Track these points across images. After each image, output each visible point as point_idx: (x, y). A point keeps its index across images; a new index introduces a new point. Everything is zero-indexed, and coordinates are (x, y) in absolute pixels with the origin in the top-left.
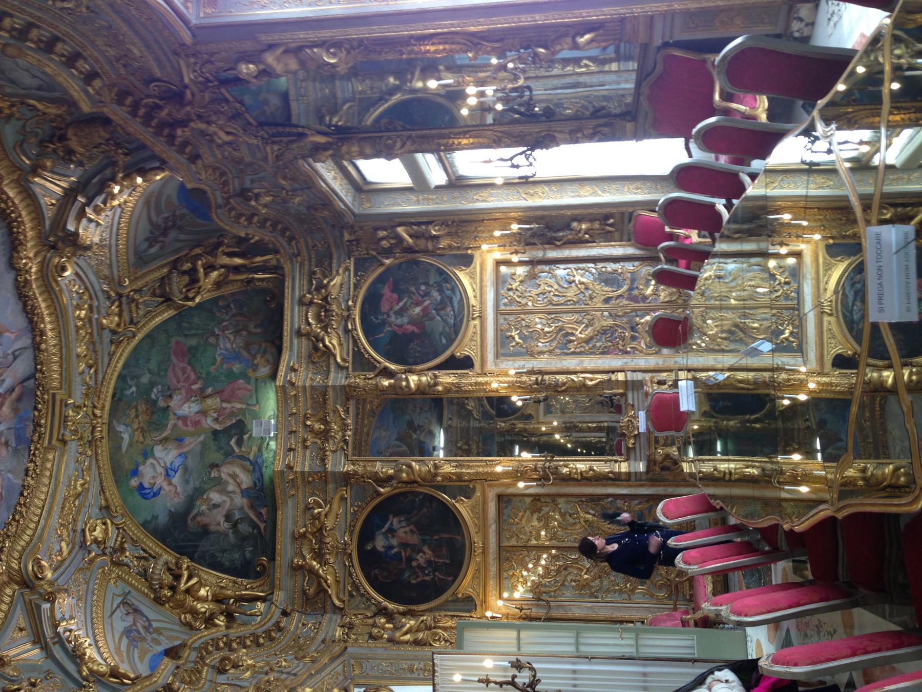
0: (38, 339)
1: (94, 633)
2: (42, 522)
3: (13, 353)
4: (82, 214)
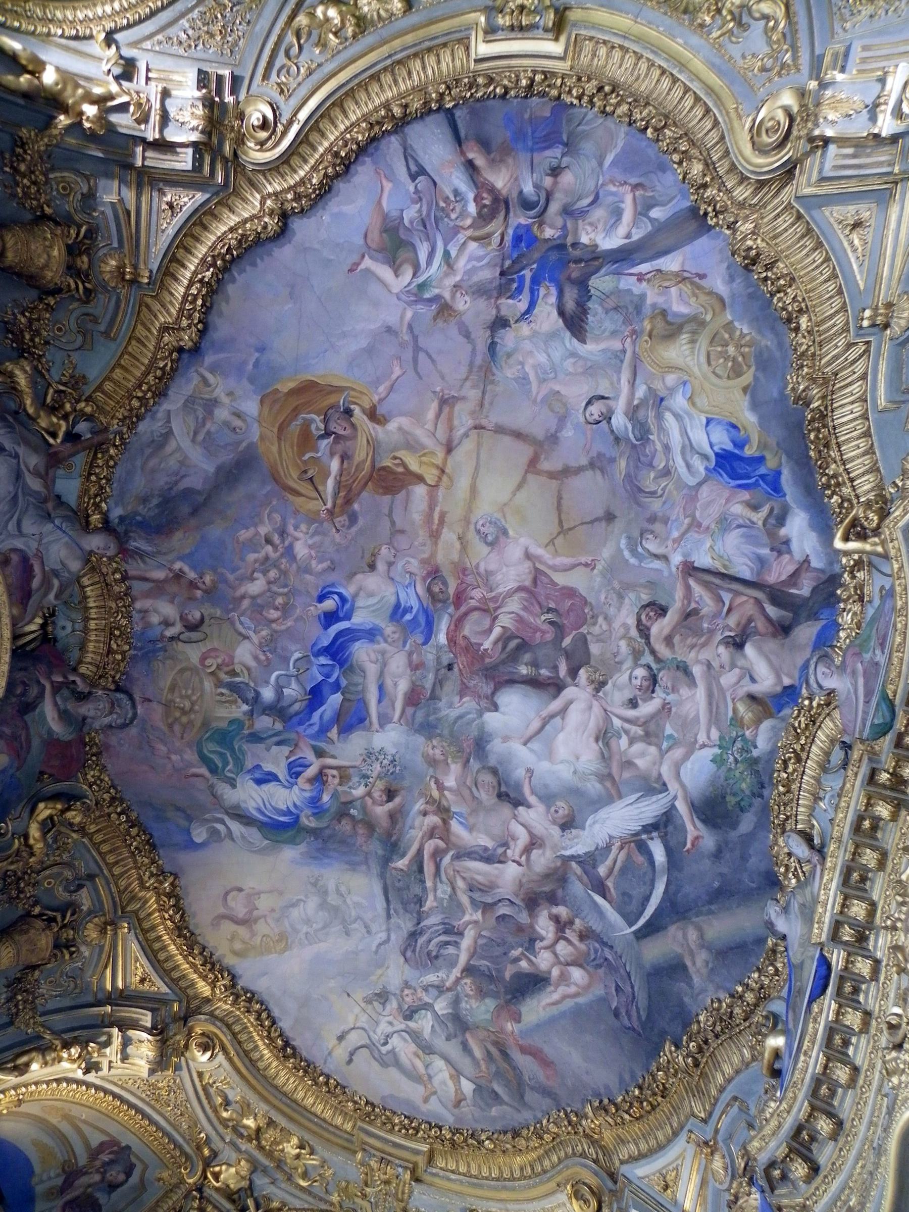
0: (387, 126)
3: (413, 177)
4: (163, 146)
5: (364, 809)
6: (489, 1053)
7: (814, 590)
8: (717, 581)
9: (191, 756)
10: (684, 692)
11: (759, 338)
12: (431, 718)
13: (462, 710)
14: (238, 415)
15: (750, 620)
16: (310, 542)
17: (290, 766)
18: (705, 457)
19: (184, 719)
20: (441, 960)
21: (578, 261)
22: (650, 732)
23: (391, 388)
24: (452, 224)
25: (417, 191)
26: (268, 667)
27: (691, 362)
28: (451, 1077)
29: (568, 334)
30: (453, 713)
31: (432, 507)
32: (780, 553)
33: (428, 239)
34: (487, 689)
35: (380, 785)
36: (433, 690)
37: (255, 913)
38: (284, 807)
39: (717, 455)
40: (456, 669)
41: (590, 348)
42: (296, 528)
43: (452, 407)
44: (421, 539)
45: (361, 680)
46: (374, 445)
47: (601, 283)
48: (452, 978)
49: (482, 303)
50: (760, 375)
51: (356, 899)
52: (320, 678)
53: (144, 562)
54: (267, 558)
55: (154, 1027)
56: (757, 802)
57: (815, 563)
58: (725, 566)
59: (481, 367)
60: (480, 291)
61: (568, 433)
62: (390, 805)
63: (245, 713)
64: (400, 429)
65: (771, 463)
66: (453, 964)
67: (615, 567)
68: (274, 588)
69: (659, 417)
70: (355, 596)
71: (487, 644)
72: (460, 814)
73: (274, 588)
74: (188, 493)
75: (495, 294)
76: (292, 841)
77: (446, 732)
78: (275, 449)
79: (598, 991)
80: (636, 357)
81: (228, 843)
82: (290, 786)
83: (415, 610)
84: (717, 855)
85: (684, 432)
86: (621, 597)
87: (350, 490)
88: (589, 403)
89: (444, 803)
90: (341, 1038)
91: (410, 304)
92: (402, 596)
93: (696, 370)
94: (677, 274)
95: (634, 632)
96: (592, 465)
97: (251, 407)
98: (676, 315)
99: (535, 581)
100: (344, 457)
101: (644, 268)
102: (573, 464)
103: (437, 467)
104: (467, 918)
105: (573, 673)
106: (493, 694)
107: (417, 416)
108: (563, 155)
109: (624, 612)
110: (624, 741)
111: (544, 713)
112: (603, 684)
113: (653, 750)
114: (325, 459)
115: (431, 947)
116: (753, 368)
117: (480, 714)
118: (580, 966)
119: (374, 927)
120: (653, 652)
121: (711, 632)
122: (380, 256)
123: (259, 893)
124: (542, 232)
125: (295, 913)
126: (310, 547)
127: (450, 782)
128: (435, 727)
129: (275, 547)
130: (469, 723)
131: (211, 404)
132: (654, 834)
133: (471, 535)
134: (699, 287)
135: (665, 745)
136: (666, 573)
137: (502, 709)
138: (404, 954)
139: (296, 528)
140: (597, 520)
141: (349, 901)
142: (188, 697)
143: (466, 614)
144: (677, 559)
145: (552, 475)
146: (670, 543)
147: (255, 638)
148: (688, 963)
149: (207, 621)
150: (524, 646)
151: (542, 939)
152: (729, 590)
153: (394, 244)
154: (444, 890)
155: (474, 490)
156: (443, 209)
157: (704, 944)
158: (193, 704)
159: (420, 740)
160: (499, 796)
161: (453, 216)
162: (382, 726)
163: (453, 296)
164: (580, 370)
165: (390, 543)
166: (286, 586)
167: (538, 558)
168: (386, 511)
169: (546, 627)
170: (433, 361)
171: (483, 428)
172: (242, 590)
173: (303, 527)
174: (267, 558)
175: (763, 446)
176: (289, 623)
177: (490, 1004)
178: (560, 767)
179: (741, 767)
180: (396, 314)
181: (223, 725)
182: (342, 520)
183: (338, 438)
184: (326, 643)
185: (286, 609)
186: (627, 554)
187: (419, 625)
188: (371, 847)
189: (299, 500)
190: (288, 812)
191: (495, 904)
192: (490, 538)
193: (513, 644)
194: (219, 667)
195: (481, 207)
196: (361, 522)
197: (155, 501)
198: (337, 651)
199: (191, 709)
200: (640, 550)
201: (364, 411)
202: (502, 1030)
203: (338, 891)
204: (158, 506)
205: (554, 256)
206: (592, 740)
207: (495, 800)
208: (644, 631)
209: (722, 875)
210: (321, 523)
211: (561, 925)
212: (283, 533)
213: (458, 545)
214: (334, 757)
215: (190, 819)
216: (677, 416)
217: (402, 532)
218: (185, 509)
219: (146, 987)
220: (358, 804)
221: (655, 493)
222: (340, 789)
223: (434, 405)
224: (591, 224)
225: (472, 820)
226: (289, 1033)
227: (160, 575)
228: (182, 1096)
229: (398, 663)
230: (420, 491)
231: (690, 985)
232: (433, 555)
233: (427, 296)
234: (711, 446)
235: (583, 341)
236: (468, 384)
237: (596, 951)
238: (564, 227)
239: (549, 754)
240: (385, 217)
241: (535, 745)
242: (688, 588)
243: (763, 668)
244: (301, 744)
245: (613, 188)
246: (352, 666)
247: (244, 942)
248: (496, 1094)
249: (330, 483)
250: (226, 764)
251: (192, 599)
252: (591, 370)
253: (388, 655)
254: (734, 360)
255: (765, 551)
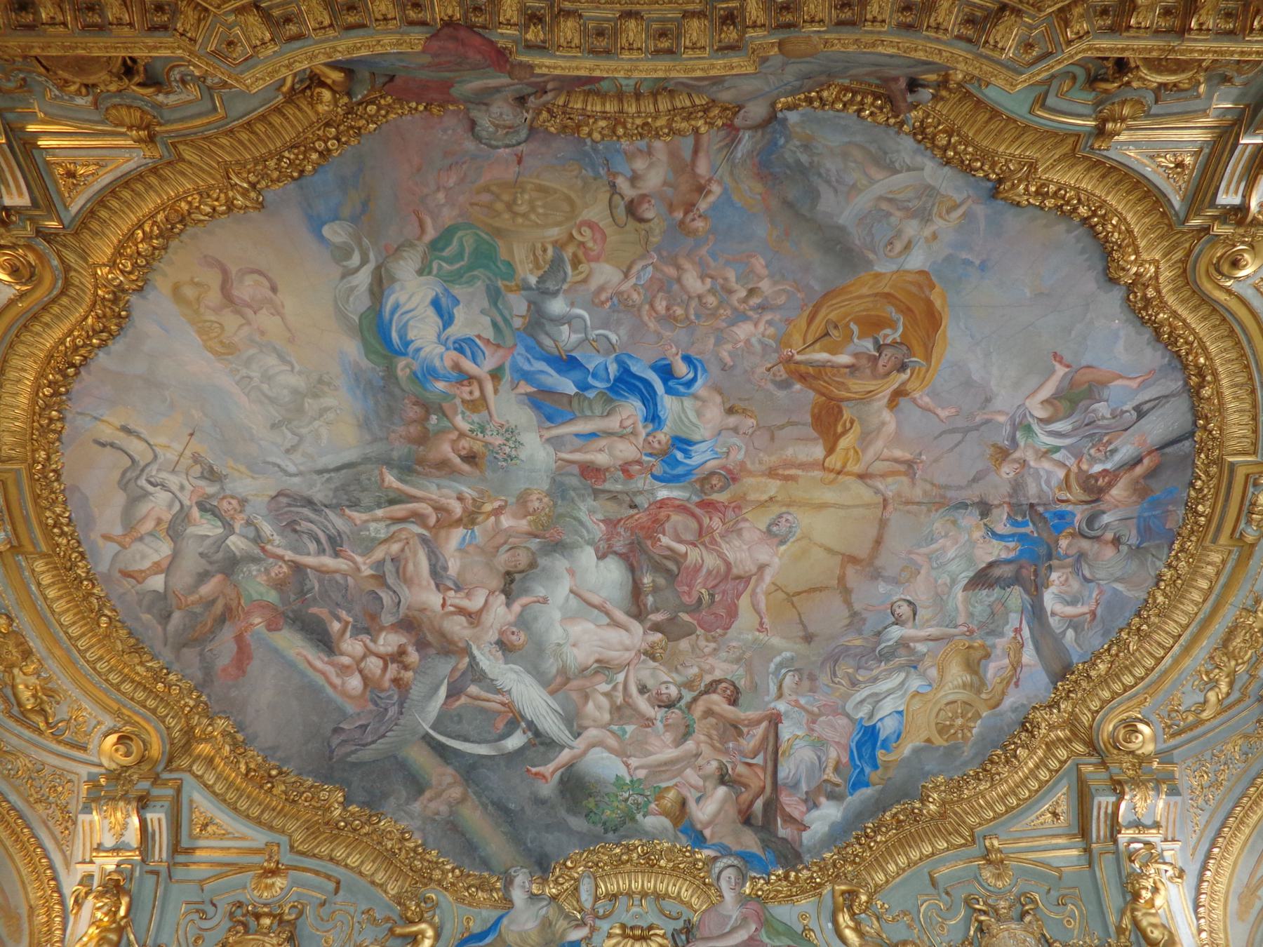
1: (1210, 851)
2: (1168, 660)
3: (1137, 408)
5: (442, 432)
6: (213, 602)
7: (783, 839)
8: (770, 748)
9: (448, 216)
10: (668, 737)
11: (970, 744)
12: (573, 494)
13: (589, 523)
14: (908, 247)
15: (746, 786)
16: (754, 340)
17: (469, 341)
18: (871, 716)
19: (499, 206)
20: (294, 536)
21: (1036, 573)
22: (622, 711)
23: (926, 409)
24: (1085, 451)
25: (1123, 412)
26: (594, 303)
27: (948, 688)
28: (157, 564)
29: (971, 574)
30: (583, 516)
31: (802, 466)
32: (806, 801)
33: (1074, 429)
34: (619, 545)
35: (477, 447)
36: (604, 491)
37: (249, 312)
38: (411, 335)
39: (874, 726)
40: (632, 512)
41: (959, 594)
42: (770, 323)
43: (906, 474)
44: (766, 458)
45: (598, 411)
46: (868, 397)
47: (1016, 597)
48: (280, 551)
49: (1006, 489)
50: (941, 751)
51: (324, 431)
52: (591, 367)
53: (721, 149)
54: (730, 292)
56: (599, 829)
57: (805, 835)
58: (784, 752)
59: (943, 497)
60: (1017, 486)
61: (882, 588)
62: (457, 461)
63: (524, 280)
64: (883, 424)
65: (874, 776)
66: (295, 550)
67: (766, 652)
68: (694, 303)
69: (900, 668)
70: (695, 397)
71: (665, 540)
72: (473, 537)
73: (694, 303)
74: (814, 196)
75: (1014, 501)
76: (368, 350)
77: (561, 510)
78: (865, 291)
79: (350, 708)
80: (950, 638)
81: (338, 271)
82: (445, 344)
83: (687, 461)
84: (540, 802)
85: (890, 693)
86: (738, 660)
87: (815, 378)
88: (910, 603)
89: (481, 518)
90: (126, 430)
91: (1012, 419)
92: (702, 447)
93: (942, 693)
94: (1019, 662)
95: (708, 679)
96: (854, 614)
97: (916, 261)
98: (986, 666)
99: (739, 578)
100: (852, 368)
101: (1026, 632)
102: (854, 597)
103: (844, 466)
104: (359, 559)
105: (656, 628)
106: (616, 553)
107: (897, 439)
108: (1130, 546)
109: (725, 666)
110: (605, 687)
111: (609, 606)
112: (654, 658)
113: (607, 717)
114: (851, 348)
115: (304, 523)
116: (946, 744)
117: (589, 543)
118: (366, 685)
119: (297, 457)
120: (695, 700)
121: (726, 752)
122: (1066, 382)
123: (279, 313)
124: (1066, 537)
125: (272, 361)
126: (748, 341)
127: (506, 522)
128: (563, 498)
129: (744, 301)
130: (577, 532)
131: (924, 216)
132: (530, 734)
133: (775, 510)
134: (1008, 683)
135: (615, 728)
136: (767, 699)
137: (601, 564)
138: (279, 494)
139: (770, 323)
140: (804, 627)
141: (316, 424)
142: (533, 209)
143: (693, 515)
144: (781, 706)
145: (842, 579)
146: (794, 697)
147: (626, 286)
148: (428, 794)
149: (643, 226)
150: (671, 576)
151: (374, 641)
152: (765, 761)
153: (1076, 396)
154: (378, 530)
155: (823, 506)
156: (1100, 440)
157: (453, 806)
158: (525, 215)
159: (546, 486)
160: (508, 573)
161: (1092, 451)
162: (548, 440)
163: (1015, 461)
164: (939, 590)
165: (759, 427)
166: (698, 316)
167: (761, 578)
168: (794, 419)
169: (695, 595)
170: (952, 449)
171: (885, 507)
172: (687, 265)
173: (771, 331)
174: (730, 292)
175: (887, 766)
176: (652, 325)
177: (272, 597)
178: (560, 630)
179: (622, 806)
180: (1004, 403)
181: (503, 254)
182: (782, 373)
183: (874, 360)
184: (634, 369)
185: (669, 319)
186: (778, 659)
187: (673, 469)
188: (397, 444)
189: (803, 323)
190: (407, 344)
191: (389, 588)
192: (775, 529)
193: (671, 566)
194: (582, 244)
195: (1096, 477)
196: (781, 394)
197: (804, 158)
198: (627, 383)
199: (515, 214)
200: (783, 671)
201: (904, 383)
202: (248, 614)
203: (323, 411)
204: (798, 162)
205: (1042, 551)
206: (597, 656)
207: (503, 570)
208: (712, 687)
209: (522, 809)
210: (776, 351)
211: (398, 656)
212: (762, 308)
213: (765, 497)
214: (496, 391)
215: (354, 219)
216: (902, 683)
217: (772, 439)
218: (792, 193)
220: (446, 423)
221: (835, 675)
222: (458, 401)
223: (908, 456)
224: (1067, 580)
225: (471, 549)
226: (93, 366)
227: (702, 168)
229: (626, 450)
230: (818, 451)
231: (407, 802)
232: (751, 474)
233: (1018, 434)
234: (881, 719)
235: (965, 589)
236: (928, 487)
237: (390, 697)
238: (1067, 556)
239: (569, 618)
240: (1104, 384)
241: (574, 602)
242: (759, 722)
243: (710, 808)
244: (501, 352)
245: (1094, 595)
246: (612, 401)
247: (198, 299)
248: (169, 616)
249: (823, 356)
250: (449, 261)
251: (671, 208)
252: (939, 599)
253: (632, 439)
254: (952, 726)
255: (804, 787)
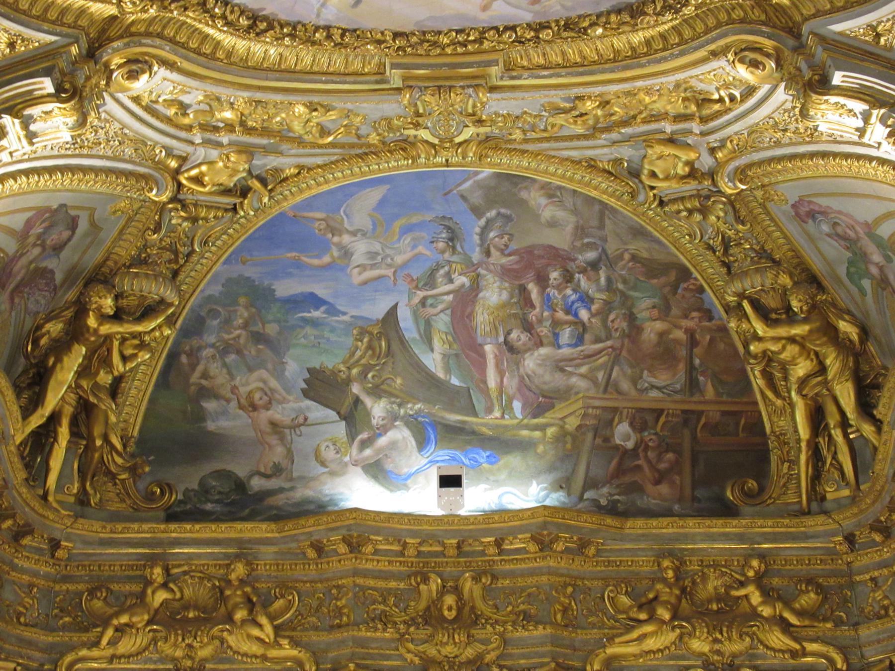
55: (59, 89)
219: (20, 48)
228: (117, 125)
